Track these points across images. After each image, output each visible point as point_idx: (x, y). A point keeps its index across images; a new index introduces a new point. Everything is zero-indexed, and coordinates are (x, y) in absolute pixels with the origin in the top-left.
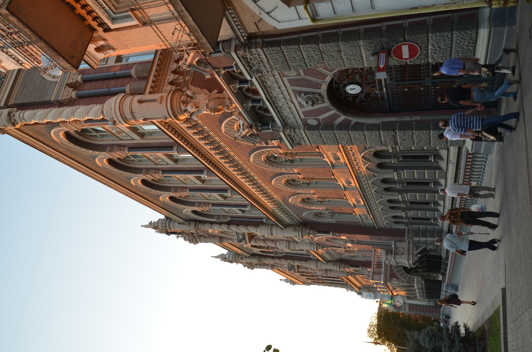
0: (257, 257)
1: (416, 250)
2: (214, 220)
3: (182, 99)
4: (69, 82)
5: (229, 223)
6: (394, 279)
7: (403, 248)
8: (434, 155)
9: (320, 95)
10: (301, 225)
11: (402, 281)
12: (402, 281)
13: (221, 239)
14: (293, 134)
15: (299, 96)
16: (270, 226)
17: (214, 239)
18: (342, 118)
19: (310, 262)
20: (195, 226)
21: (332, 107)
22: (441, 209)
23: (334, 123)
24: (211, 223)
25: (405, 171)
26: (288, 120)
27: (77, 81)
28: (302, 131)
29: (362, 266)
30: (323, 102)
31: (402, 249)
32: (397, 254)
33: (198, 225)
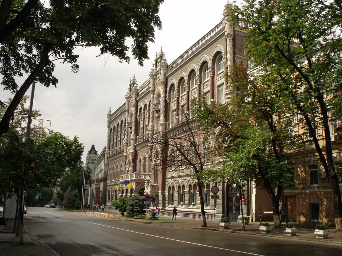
0: (136, 104)
1: (155, 196)
2: (167, 94)
5: (166, 101)
22: (180, 206)
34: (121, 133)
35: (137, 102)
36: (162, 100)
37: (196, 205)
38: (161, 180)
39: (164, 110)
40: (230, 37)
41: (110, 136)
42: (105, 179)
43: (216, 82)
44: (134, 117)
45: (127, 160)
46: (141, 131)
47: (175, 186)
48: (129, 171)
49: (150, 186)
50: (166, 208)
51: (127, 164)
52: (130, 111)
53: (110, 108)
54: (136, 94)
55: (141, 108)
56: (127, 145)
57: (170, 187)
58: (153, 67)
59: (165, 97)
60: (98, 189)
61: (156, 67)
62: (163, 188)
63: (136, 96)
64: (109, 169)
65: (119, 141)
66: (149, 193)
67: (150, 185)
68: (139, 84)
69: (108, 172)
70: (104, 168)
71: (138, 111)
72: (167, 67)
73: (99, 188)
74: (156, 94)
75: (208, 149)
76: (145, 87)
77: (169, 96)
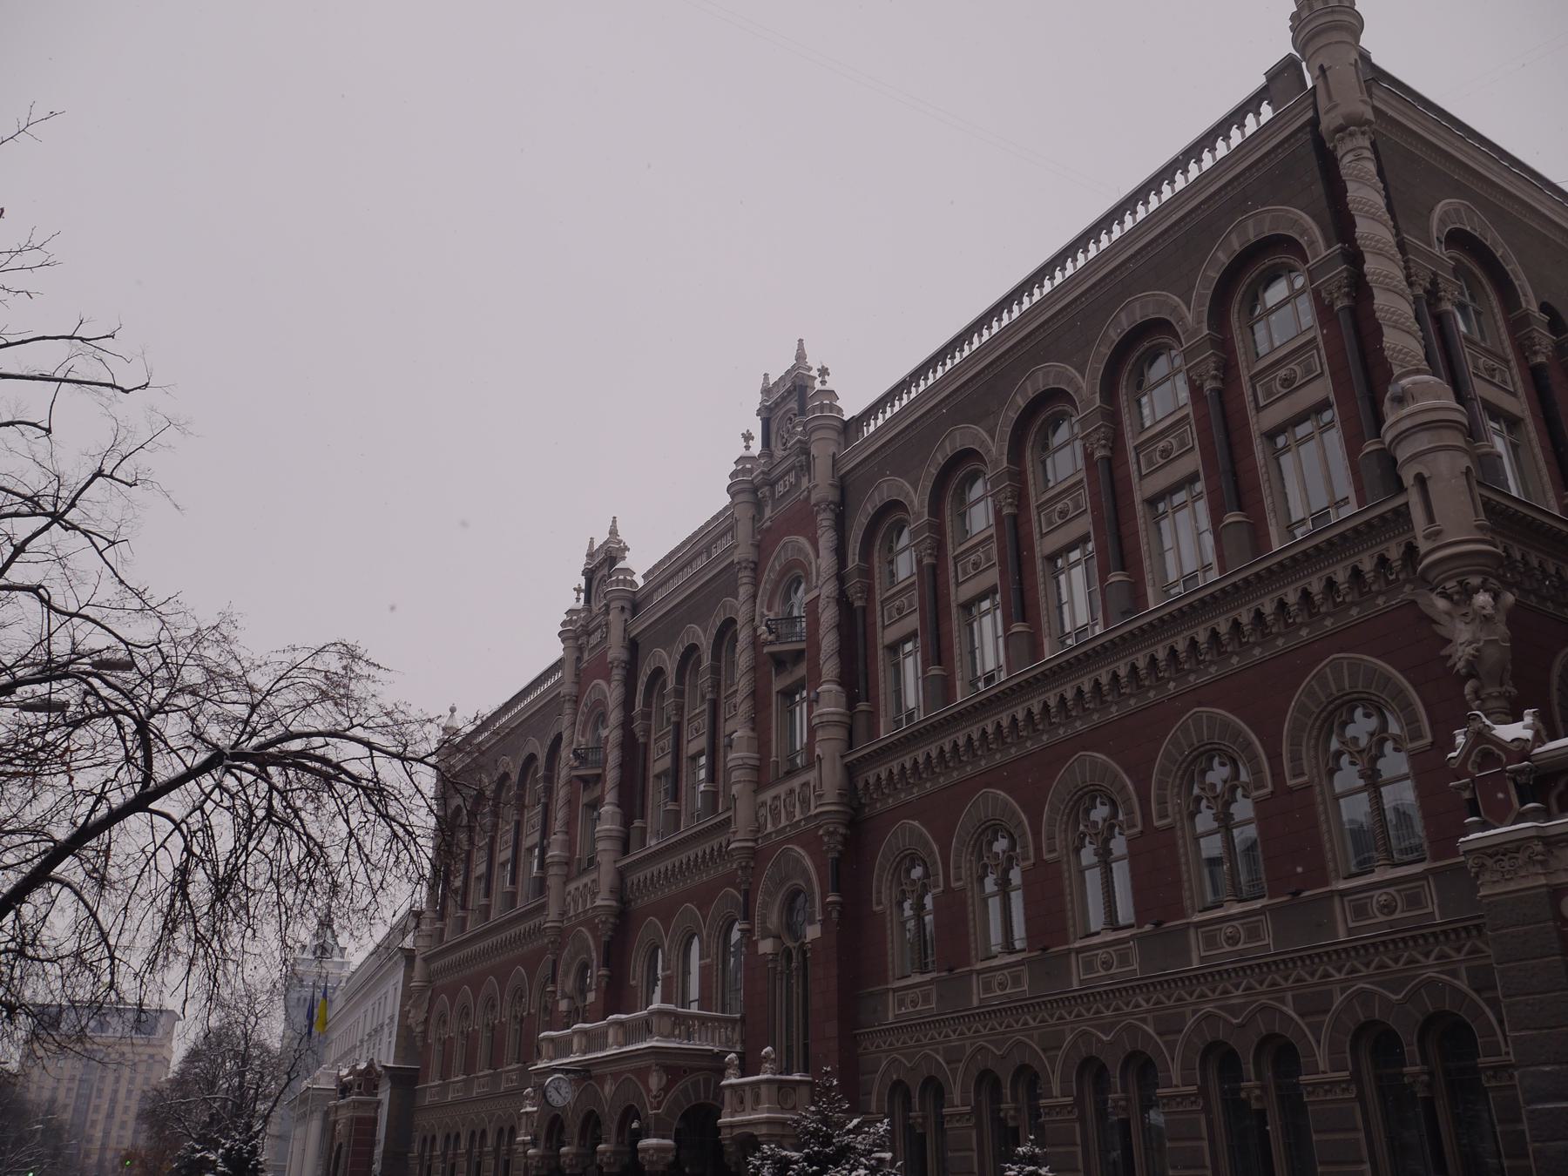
2: (853, 561)
3: (1491, 580)
4: (1440, 280)
5: (842, 601)
10: (853, 809)
11: (659, 1104)
13: (752, 565)
14: (1522, 857)
17: (752, 544)
19: (618, 818)
20: (831, 502)
24: (840, 552)
27: (1440, 299)
28: (1543, 881)
29: (609, 977)
32: (779, 1089)
33: (832, 510)
34: (518, 824)
35: (633, 646)
40: (1359, 136)
43: (1251, 412)
44: (614, 717)
46: (656, 796)
54: (627, 605)
55: (658, 672)
58: (747, 447)
59: (841, 577)
63: (627, 615)
65: (479, 878)
68: (640, 562)
69: (425, 1033)
70: (404, 1015)
71: (641, 688)
73: (374, 1121)
74: (769, 576)
76: (689, 563)
77: (866, 573)
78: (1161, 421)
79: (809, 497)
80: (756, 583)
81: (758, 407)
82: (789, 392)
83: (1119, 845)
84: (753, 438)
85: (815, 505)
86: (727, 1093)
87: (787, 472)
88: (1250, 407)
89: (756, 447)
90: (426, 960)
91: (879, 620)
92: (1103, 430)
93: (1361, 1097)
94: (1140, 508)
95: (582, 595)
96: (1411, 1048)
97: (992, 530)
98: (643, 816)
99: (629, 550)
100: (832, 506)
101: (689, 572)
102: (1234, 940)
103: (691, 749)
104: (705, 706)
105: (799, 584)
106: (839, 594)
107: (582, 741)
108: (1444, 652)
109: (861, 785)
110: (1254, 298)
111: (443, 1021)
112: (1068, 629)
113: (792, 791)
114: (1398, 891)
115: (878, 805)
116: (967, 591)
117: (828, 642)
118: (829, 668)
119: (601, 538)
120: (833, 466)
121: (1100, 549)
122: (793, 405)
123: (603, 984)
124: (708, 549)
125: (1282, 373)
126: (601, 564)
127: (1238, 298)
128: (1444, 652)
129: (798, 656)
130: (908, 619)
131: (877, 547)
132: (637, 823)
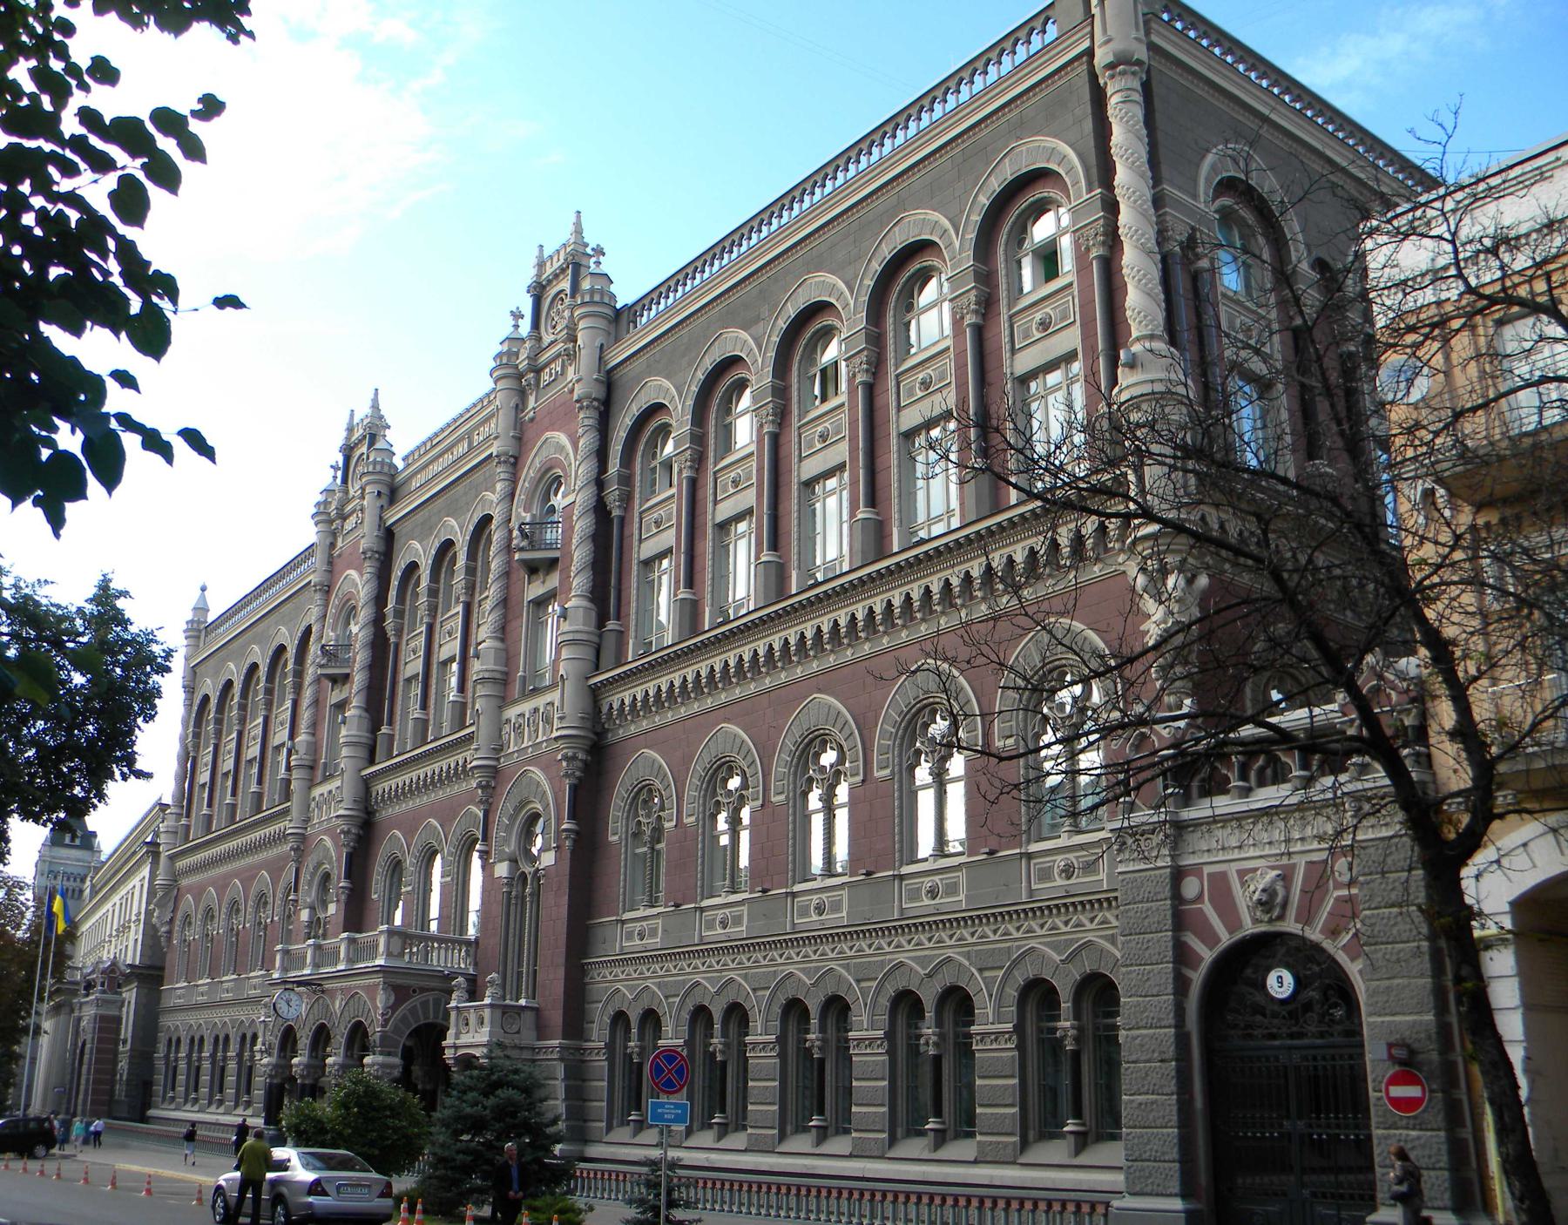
0: (382, 548)
2: (614, 467)
5: (600, 509)
6: (392, 998)
7: (518, 1032)
8: (825, 1128)
9: (1281, 917)
10: (596, 734)
12: (386, 1022)
13: (512, 460)
15: (1278, 876)
16: (596, 639)
18: (1207, 955)
20: (595, 399)
21: (1239, 936)
23: (1189, 933)
24: (602, 455)
25: (886, 1058)
26: (1199, 834)
29: (351, 890)
30: (1256, 921)
31: (515, 1028)
32: (504, 1013)
33: (596, 408)
35: (389, 536)
36: (572, 498)
37: (744, 1128)
38: (561, 972)
39: (589, 558)
41: (197, 735)
42: (150, 975)
43: (1006, 355)
44: (364, 614)
45: (310, 862)
47: (663, 1010)
48: (314, 923)
49: (487, 1013)
50: (595, 1151)
51: (303, 886)
52: (341, 588)
53: (203, 589)
54: (385, 490)
55: (413, 567)
56: (311, 780)
57: (620, 1018)
58: (516, 326)
59: (600, 483)
60: (108, 1026)
61: (536, 324)
62: (575, 1024)
63: (384, 501)
64: (179, 915)
66: (477, 1052)
67: (487, 1001)
68: (403, 440)
69: (170, 932)
70: (149, 913)
71: (395, 583)
72: (620, 319)
73: (118, 1020)
74: (529, 473)
75: (652, 837)
76: (449, 449)
77: (626, 480)
78: (926, 349)
79: (572, 391)
80: (514, 480)
81: (529, 282)
82: (563, 270)
83: (842, 792)
84: (522, 317)
85: (577, 401)
86: (453, 1014)
87: (554, 360)
88: (1006, 347)
89: (525, 327)
90: (172, 858)
91: (636, 532)
92: (865, 353)
93: (1021, 1047)
94: (894, 441)
95: (339, 474)
96: (1066, 1005)
97: (753, 448)
98: (390, 723)
99: (389, 427)
100: (595, 404)
101: (449, 458)
102: (933, 893)
103: (444, 653)
104: (423, 628)
105: (560, 484)
106: (597, 501)
107: (330, 636)
108: (1143, 628)
109: (605, 709)
110: (1021, 230)
111: (187, 920)
112: (818, 562)
113: (536, 710)
114: (1077, 858)
115: (621, 731)
116: (725, 511)
117: (580, 554)
118: (579, 582)
119: (363, 411)
120: (600, 358)
121: (854, 483)
122: (565, 284)
123: (343, 897)
124: (469, 435)
125: (1038, 316)
126: (360, 441)
127: (1005, 230)
128: (1143, 628)
129: (552, 564)
130: (665, 534)
131: (639, 454)
132: (384, 729)
